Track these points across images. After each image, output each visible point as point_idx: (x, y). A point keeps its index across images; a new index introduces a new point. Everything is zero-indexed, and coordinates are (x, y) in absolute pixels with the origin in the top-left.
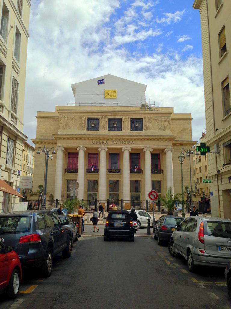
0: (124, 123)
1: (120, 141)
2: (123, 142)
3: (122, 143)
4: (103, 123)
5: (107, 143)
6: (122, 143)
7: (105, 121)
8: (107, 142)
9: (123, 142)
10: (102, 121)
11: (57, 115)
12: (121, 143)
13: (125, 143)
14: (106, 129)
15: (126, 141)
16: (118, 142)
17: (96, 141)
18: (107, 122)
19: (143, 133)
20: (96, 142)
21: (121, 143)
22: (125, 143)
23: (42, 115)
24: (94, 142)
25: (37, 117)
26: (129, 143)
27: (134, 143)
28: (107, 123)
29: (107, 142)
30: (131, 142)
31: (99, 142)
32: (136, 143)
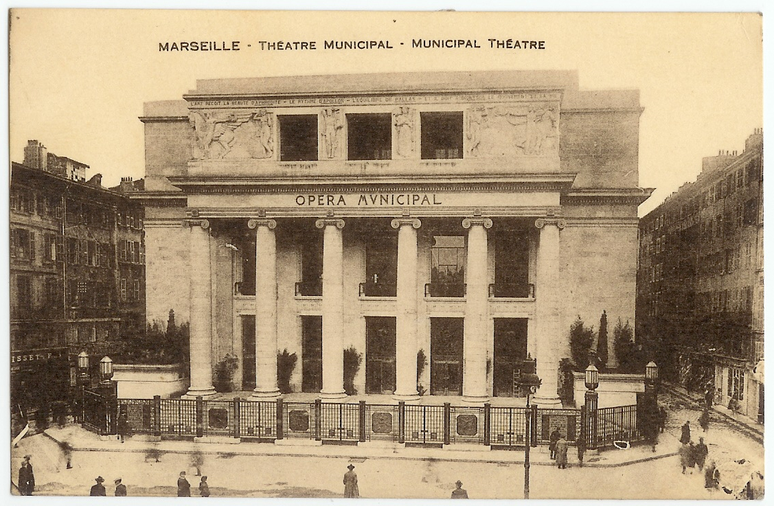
3: (390, 200)
5: (342, 203)
7: (336, 127)
8: (341, 199)
11: (182, 111)
12: (387, 201)
13: (401, 200)
14: (338, 154)
15: (406, 195)
16: (378, 199)
17: (306, 197)
18: (340, 128)
19: (463, 166)
20: (307, 201)
21: (387, 201)
22: (401, 200)
23: (156, 113)
25: (145, 120)
29: (341, 199)
30: (421, 200)
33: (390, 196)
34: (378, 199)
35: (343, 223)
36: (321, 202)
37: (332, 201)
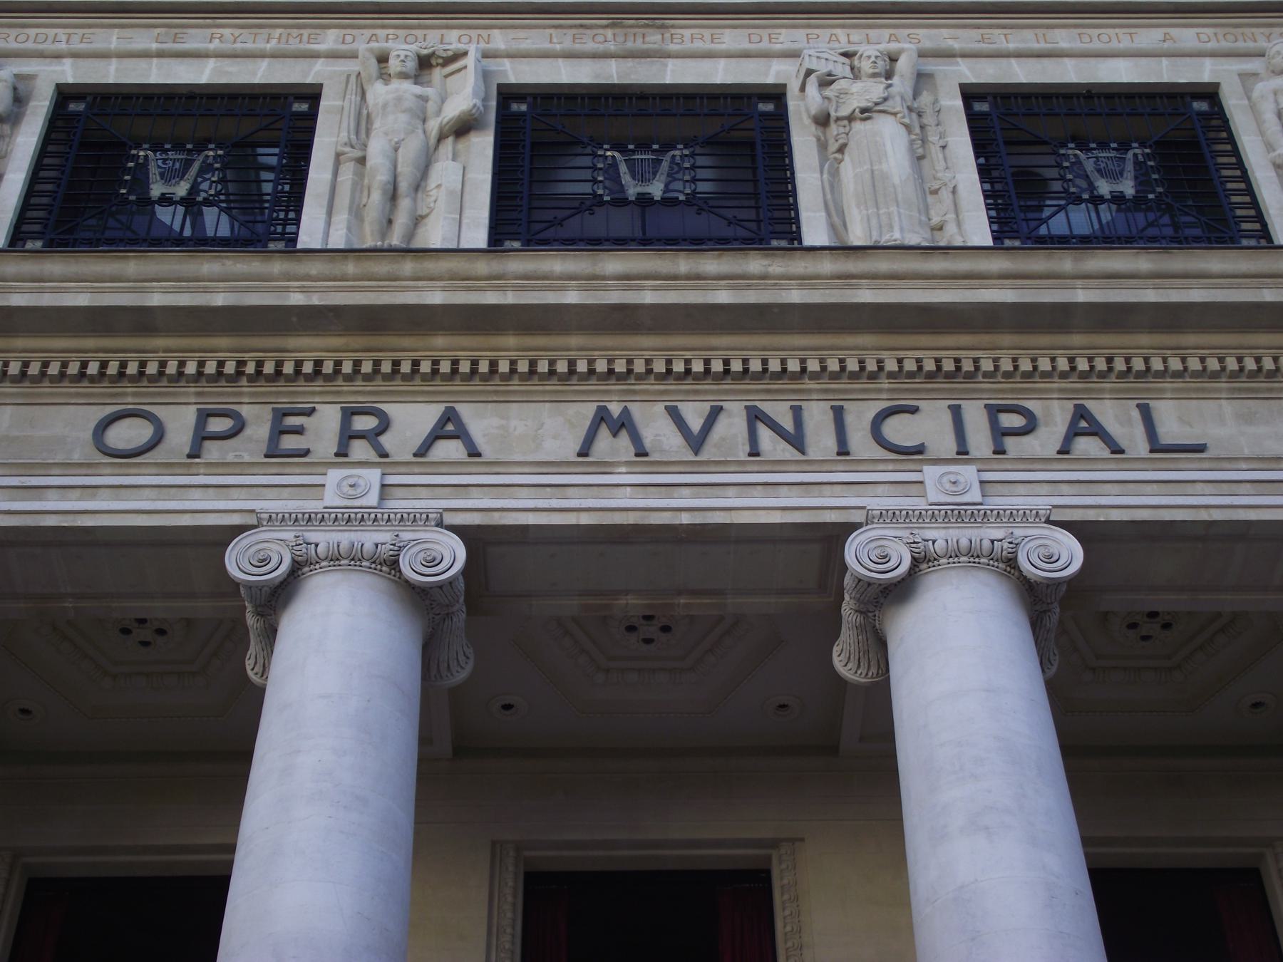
0: (831, 155)
1: (780, 412)
2: (860, 416)
3: (821, 441)
4: (377, 149)
5: (449, 450)
6: (821, 441)
9: (860, 416)
10: (363, 123)
12: (796, 440)
13: (900, 430)
16: (732, 425)
18: (463, 128)
21: (796, 440)
24: (128, 434)
26: (1000, 434)
27: (1137, 444)
28: (483, 146)
31: (259, 428)
32: (1172, 427)
33: (817, 416)
34: (732, 425)
35: (454, 552)
36: (289, 442)
37: (372, 437)
